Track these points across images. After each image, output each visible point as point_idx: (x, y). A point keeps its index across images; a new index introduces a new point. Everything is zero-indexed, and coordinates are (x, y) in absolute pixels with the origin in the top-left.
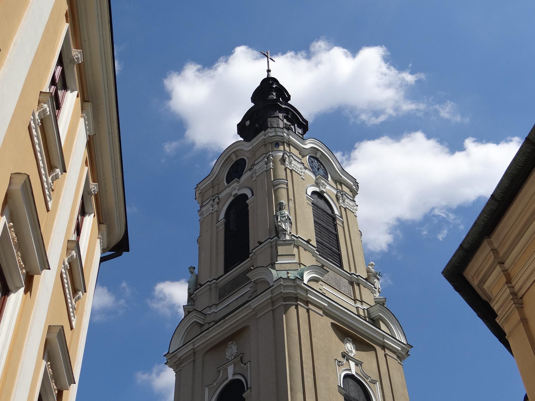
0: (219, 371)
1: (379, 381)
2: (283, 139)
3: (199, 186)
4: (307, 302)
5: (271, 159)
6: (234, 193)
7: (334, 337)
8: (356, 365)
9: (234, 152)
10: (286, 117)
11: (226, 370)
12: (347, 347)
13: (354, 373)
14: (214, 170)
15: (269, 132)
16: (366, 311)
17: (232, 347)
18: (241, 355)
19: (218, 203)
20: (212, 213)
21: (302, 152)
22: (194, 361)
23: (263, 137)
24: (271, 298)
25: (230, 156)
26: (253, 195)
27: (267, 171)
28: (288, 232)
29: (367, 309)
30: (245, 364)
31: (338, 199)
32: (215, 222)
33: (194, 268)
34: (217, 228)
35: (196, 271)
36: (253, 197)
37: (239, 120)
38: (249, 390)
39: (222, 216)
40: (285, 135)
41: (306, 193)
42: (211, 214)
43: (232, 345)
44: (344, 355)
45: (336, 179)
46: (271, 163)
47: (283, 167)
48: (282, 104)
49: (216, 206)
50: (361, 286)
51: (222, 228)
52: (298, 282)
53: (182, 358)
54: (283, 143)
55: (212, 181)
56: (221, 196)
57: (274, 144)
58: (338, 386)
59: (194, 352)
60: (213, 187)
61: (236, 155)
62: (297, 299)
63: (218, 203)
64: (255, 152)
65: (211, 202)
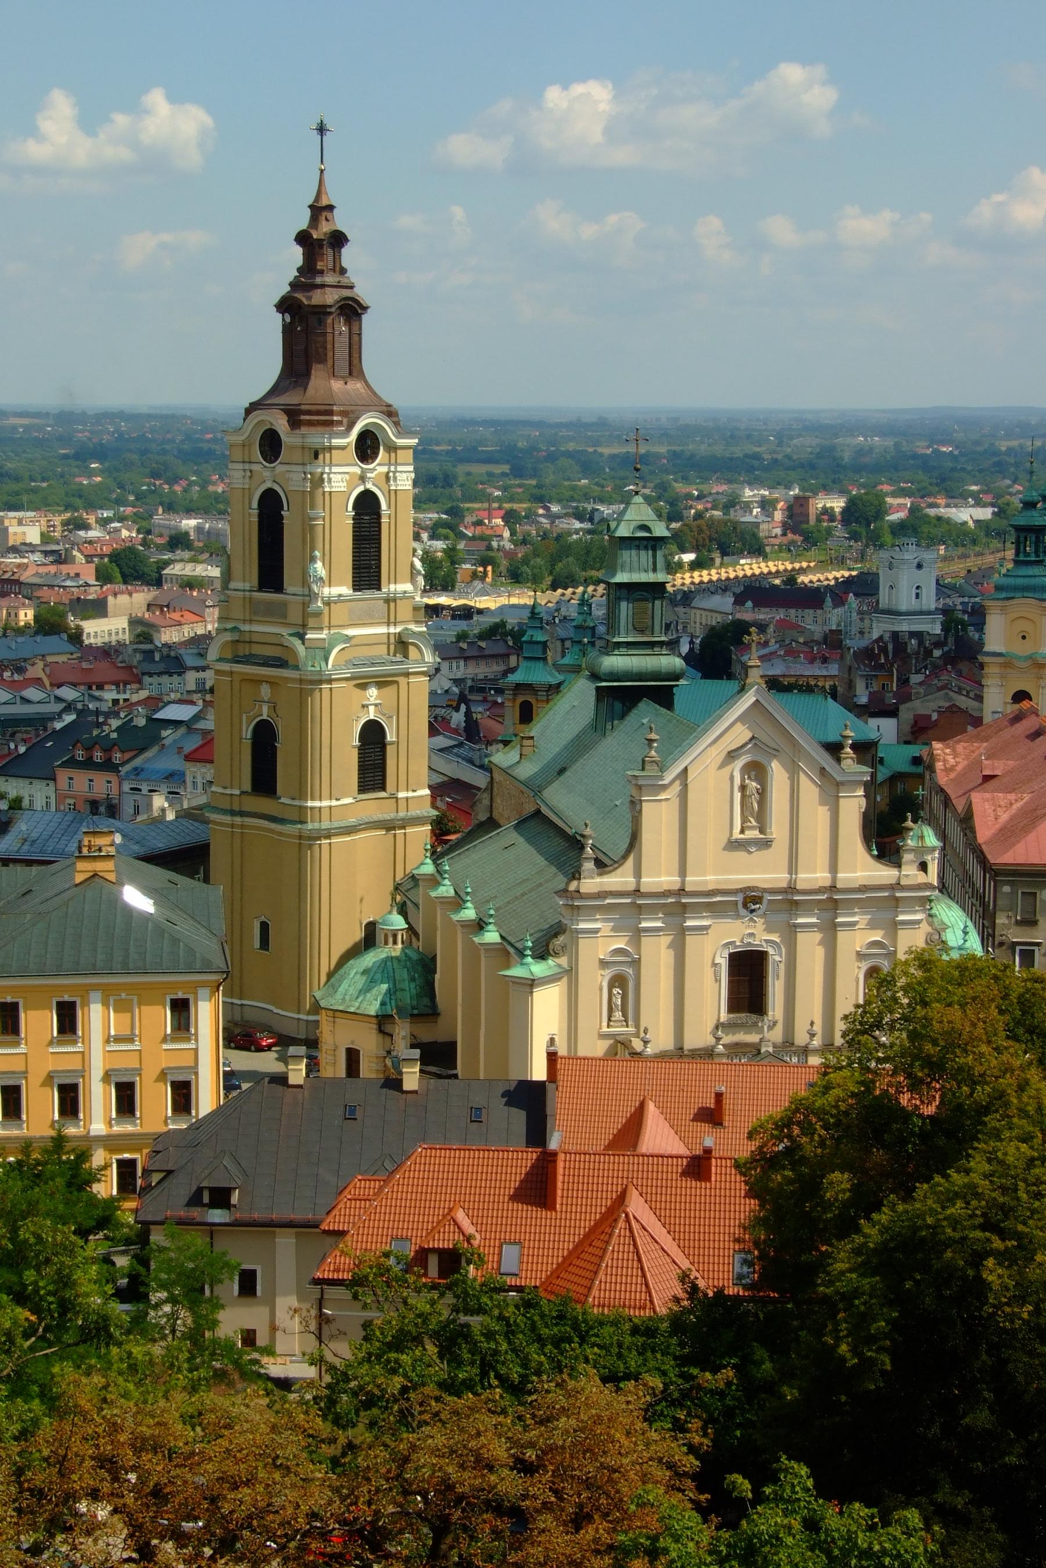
13: (372, 717)
31: (388, 478)
39: (255, 505)
49: (247, 480)
51: (255, 519)
62: (321, 682)
65: (242, 473)
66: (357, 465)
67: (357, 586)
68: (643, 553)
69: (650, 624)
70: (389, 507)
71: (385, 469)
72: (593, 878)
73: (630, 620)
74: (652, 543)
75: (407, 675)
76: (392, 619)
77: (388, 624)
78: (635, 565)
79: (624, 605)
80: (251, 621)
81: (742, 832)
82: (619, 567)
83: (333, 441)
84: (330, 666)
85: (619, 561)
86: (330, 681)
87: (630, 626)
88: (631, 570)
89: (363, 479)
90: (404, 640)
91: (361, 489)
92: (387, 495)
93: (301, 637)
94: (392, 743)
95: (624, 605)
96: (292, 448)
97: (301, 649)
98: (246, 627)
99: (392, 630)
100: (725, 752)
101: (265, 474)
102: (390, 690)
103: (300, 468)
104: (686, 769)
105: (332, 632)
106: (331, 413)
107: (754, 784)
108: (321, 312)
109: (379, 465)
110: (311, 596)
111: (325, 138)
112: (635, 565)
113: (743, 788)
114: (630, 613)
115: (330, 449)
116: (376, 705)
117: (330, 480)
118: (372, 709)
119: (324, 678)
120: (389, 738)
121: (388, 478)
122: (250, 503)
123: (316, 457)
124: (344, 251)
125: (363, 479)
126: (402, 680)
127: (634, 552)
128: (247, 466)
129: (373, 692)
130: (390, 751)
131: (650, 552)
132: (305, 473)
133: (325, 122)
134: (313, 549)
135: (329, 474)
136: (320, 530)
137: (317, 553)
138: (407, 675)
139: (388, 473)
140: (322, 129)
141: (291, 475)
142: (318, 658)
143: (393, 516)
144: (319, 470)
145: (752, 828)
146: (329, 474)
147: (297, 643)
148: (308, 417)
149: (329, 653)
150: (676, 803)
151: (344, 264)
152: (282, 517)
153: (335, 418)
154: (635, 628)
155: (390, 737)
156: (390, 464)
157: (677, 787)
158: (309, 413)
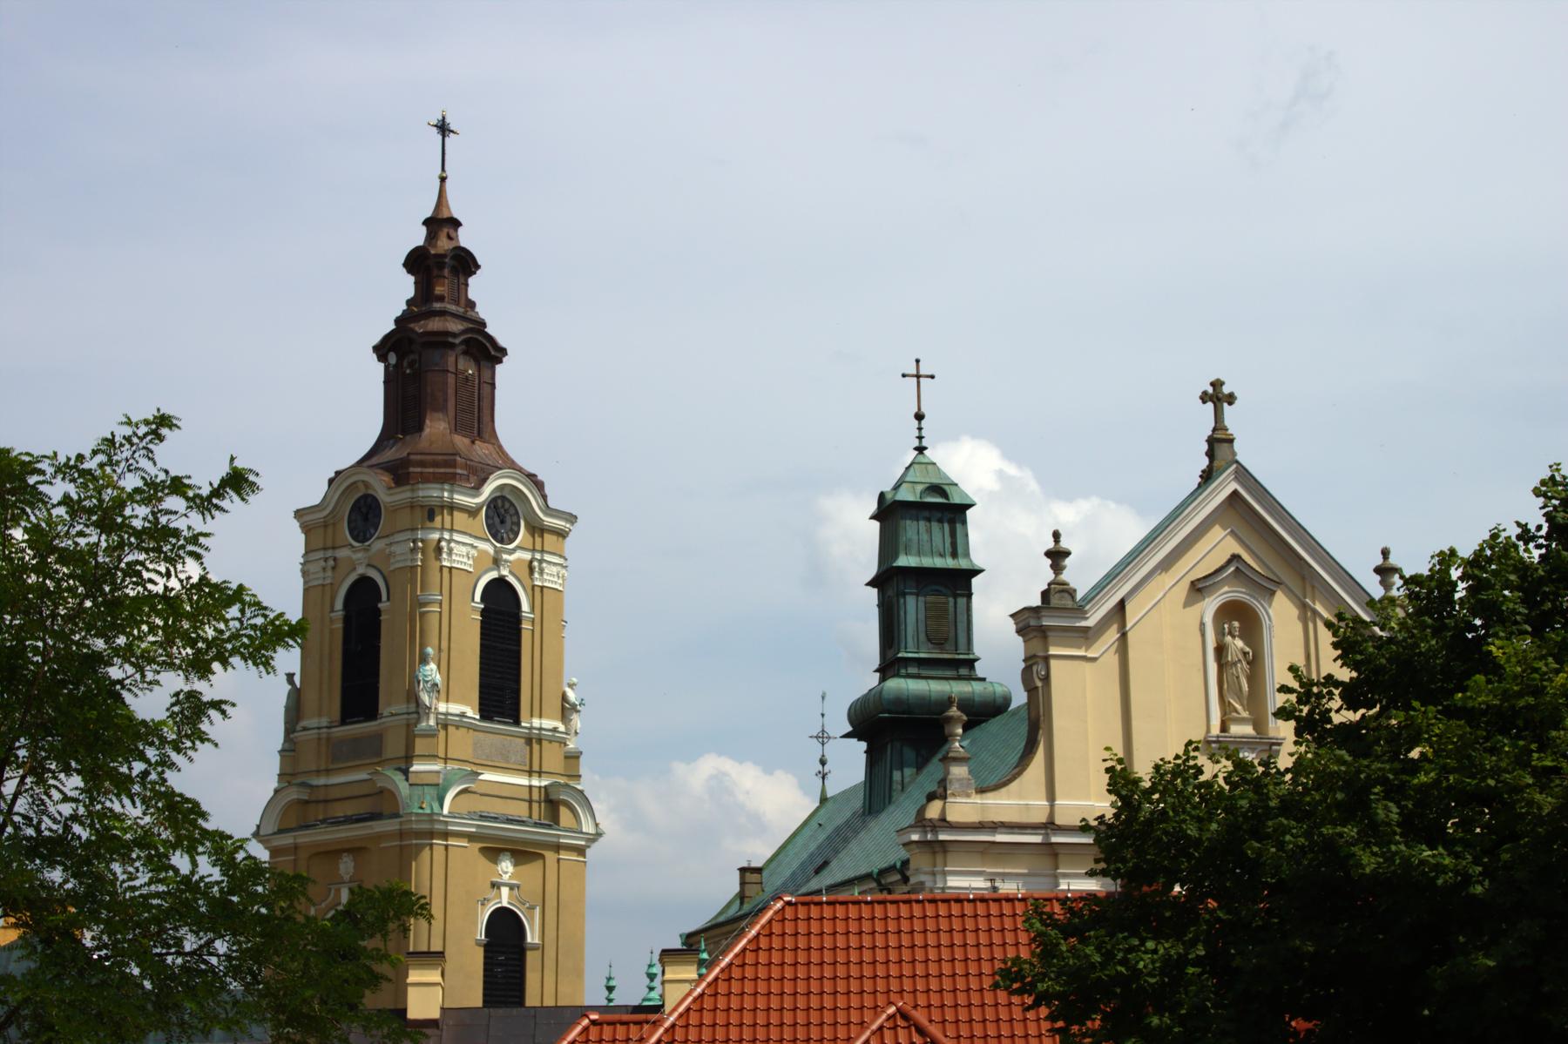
0: (330, 889)
4: (446, 835)
5: (419, 548)
7: (483, 862)
11: (338, 891)
13: (505, 904)
14: (328, 500)
15: (419, 489)
16: (543, 790)
20: (323, 585)
21: (472, 512)
22: (295, 860)
25: (355, 483)
26: (388, 599)
27: (411, 567)
29: (545, 787)
33: (294, 674)
36: (388, 604)
39: (339, 604)
40: (446, 494)
46: (420, 556)
49: (329, 573)
50: (545, 743)
51: (339, 625)
52: (435, 818)
54: (442, 507)
59: (296, 848)
60: (326, 526)
62: (432, 834)
65: (322, 563)
66: (488, 540)
67: (487, 712)
68: (935, 526)
69: (952, 634)
70: (533, 610)
71: (527, 556)
72: (968, 796)
73: (922, 628)
74: (948, 515)
75: (558, 848)
76: (536, 767)
77: (530, 773)
78: (927, 547)
79: (911, 601)
80: (328, 772)
81: (1224, 728)
82: (901, 547)
83: (456, 496)
84: (446, 811)
85: (903, 540)
86: (446, 835)
87: (922, 637)
88: (919, 554)
89: (497, 562)
90: (553, 797)
91: (493, 575)
92: (530, 592)
93: (406, 772)
94: (534, 947)
95: (911, 601)
96: (396, 509)
97: (403, 787)
98: (322, 781)
99: (535, 782)
100: (1186, 584)
101: (355, 557)
102: (533, 869)
103: (408, 535)
104: (1122, 605)
105: (449, 767)
106: (453, 465)
107: (1239, 643)
108: (441, 341)
109: (518, 547)
110: (420, 710)
111: (447, 139)
112: (927, 547)
113: (1220, 650)
114: (922, 616)
115: (452, 507)
116: (512, 887)
117: (450, 551)
118: (505, 891)
119: (438, 826)
120: (529, 940)
121: (531, 570)
123: (431, 517)
124: (472, 280)
125: (497, 562)
126: (550, 856)
127: (922, 523)
128: (329, 553)
129: (506, 867)
130: (532, 959)
131: (946, 526)
132: (414, 541)
133: (447, 121)
134: (423, 646)
135: (449, 542)
137: (430, 650)
138: (558, 848)
139: (531, 562)
140: (443, 128)
141: (393, 548)
142: (428, 798)
143: (537, 621)
144: (436, 536)
145: (1242, 721)
146: (449, 542)
147: (398, 778)
148: (419, 457)
149: (445, 790)
150: (1112, 660)
151: (471, 295)
152: (378, 612)
153: (459, 471)
154: (929, 640)
155: (532, 937)
156: (534, 550)
157: (1112, 635)
158: (422, 464)
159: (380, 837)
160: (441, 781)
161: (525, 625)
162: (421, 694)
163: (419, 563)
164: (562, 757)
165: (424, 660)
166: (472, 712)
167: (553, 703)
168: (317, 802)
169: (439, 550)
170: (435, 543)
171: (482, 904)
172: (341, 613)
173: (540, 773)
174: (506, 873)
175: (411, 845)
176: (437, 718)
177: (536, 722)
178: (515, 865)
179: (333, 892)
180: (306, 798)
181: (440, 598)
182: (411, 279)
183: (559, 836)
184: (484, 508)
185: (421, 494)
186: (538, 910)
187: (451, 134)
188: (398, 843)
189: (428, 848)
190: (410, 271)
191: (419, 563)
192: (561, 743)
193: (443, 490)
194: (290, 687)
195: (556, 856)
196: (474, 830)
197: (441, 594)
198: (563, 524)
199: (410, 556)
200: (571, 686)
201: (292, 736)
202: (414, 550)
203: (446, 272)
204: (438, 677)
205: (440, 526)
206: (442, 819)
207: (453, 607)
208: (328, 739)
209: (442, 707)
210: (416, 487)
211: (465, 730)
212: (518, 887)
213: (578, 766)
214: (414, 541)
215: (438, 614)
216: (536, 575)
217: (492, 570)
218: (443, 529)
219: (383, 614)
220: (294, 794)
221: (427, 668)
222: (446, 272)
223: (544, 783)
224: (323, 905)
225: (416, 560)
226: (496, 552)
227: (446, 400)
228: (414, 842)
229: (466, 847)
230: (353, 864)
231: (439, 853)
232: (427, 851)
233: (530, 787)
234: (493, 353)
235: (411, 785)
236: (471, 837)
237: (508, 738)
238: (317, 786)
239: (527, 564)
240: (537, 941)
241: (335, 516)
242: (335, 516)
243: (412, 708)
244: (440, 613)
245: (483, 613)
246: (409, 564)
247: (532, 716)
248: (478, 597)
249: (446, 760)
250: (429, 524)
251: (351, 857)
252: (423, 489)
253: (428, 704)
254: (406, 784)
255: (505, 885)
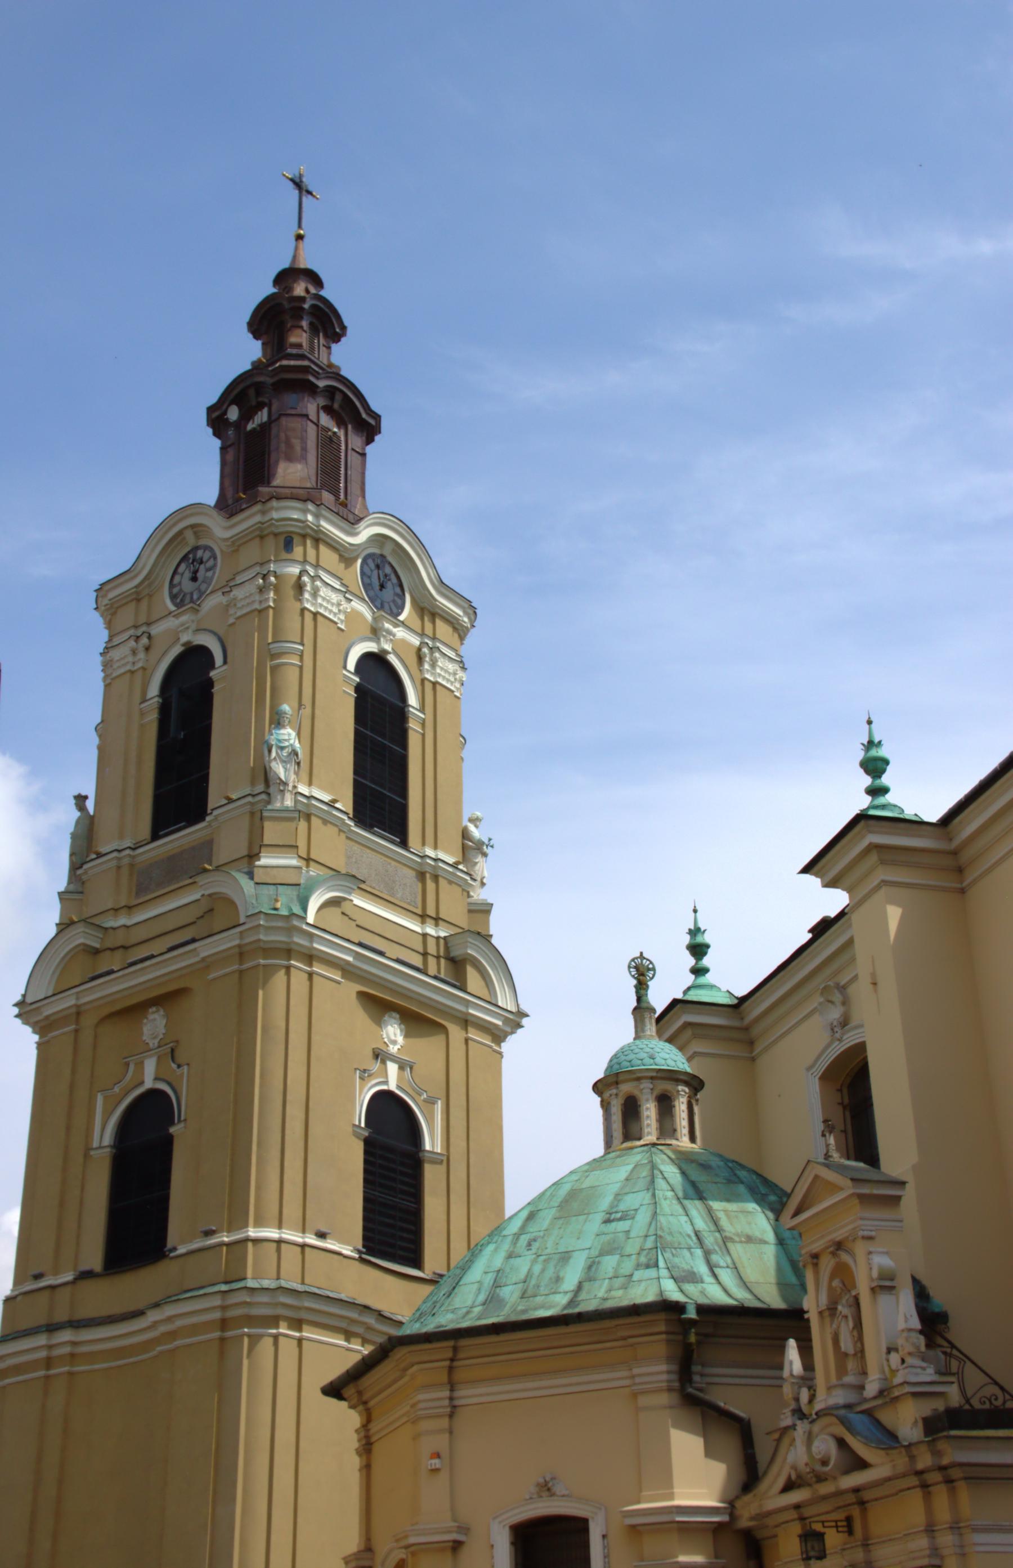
0: (127, 1064)
1: (444, 1099)
2: (302, 528)
3: (106, 588)
4: (310, 957)
5: (271, 584)
6: (185, 638)
7: (360, 1017)
8: (401, 1068)
9: (192, 526)
10: (328, 410)
11: (140, 1065)
12: (387, 1034)
13: (392, 1086)
15: (272, 508)
16: (442, 942)
17: (155, 1019)
18: (172, 1044)
19: (147, 649)
20: (132, 672)
21: (346, 555)
22: (76, 1031)
23: (258, 518)
24: (239, 946)
25: (180, 533)
26: (225, 662)
27: (260, 611)
28: (290, 788)
29: (445, 938)
30: (179, 1066)
31: (420, 659)
32: (137, 698)
33: (86, 797)
34: (142, 714)
35: (90, 805)
36: (225, 667)
37: (213, 399)
38: (182, 1125)
39: (154, 689)
40: (310, 518)
41: (345, 667)
42: (128, 675)
43: (156, 1016)
44: (376, 1053)
45: (422, 605)
46: (272, 594)
47: (297, 606)
48: (318, 378)
49: (142, 655)
50: (442, 882)
51: (153, 716)
52: (296, 922)
53: (52, 1018)
54: (304, 536)
55: (136, 587)
56: (155, 630)
57: (282, 539)
58: (354, 1125)
59: (78, 1013)
61: (195, 533)
62: (288, 952)
63: (147, 649)
64: (239, 546)
65: (132, 643)
70: (422, 710)
77: (423, 917)
83: (323, 523)
90: (455, 953)
91: (371, 647)
94: (436, 1160)
98: (123, 920)
99: (430, 930)
115: (319, 539)
120: (428, 1146)
121: (420, 659)
122: (144, 692)
123: (288, 545)
126: (455, 1032)
128: (144, 628)
129: (393, 1034)
130: (432, 1176)
132: (264, 577)
136: (291, 676)
137: (286, 708)
138: (466, 1022)
139: (419, 649)
143: (429, 724)
144: (295, 570)
152: (210, 683)
155: (432, 1142)
159: (207, 965)
160: (302, 881)
161: (413, 725)
162: (273, 765)
163: (271, 604)
164: (466, 911)
165: (278, 722)
166: (346, 803)
167: (451, 837)
168: (112, 950)
169: (300, 587)
170: (294, 579)
171: (362, 1078)
172: (156, 699)
173: (437, 920)
174: (395, 1042)
175: (258, 965)
176: (296, 801)
177: (430, 852)
178: (407, 1036)
179: (132, 1067)
180: (97, 946)
181: (301, 648)
182: (258, 345)
183: (467, 1003)
184: (359, 561)
185: (275, 515)
186: (439, 1106)
187: (310, 197)
188: (235, 967)
189: (283, 972)
190: (256, 337)
191: (271, 604)
192: (463, 890)
193: (305, 511)
194: (78, 814)
195: (463, 1034)
196: (350, 959)
197: (302, 644)
198: (460, 613)
199: (257, 597)
200: (475, 821)
201: (79, 872)
202: (261, 590)
203: (304, 324)
204: (297, 745)
205: (301, 559)
206: (304, 927)
207: (318, 663)
208: (132, 866)
209: (303, 789)
210: (269, 505)
211: (336, 829)
212: (411, 1068)
213: (487, 923)
214: (264, 577)
215: (297, 670)
216: (426, 666)
217: (370, 639)
218: (305, 561)
219: (215, 684)
220: (80, 936)
221: (282, 731)
222: (304, 324)
223: (443, 934)
224: (117, 1089)
225: (267, 600)
226: (375, 619)
227: (304, 449)
228: (262, 962)
229: (339, 983)
230: (164, 1021)
231: (299, 980)
232: (281, 976)
233: (425, 935)
234: (364, 416)
235: (257, 883)
236: (347, 971)
237: (393, 863)
238: (114, 929)
239: (415, 650)
240: (438, 1149)
241: (150, 585)
242: (150, 585)
243: (260, 787)
244: (301, 668)
245: (358, 689)
246: (257, 606)
247: (424, 844)
248: (351, 665)
249: (308, 860)
250: (284, 555)
251: (162, 1012)
252: (277, 509)
253: (283, 777)
254: (252, 883)
255: (394, 1059)
